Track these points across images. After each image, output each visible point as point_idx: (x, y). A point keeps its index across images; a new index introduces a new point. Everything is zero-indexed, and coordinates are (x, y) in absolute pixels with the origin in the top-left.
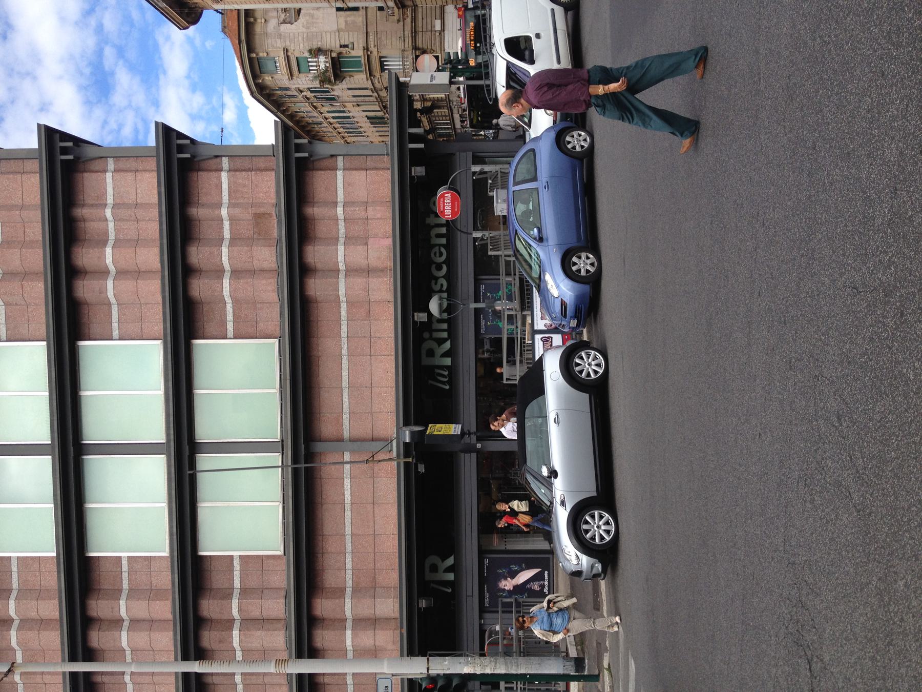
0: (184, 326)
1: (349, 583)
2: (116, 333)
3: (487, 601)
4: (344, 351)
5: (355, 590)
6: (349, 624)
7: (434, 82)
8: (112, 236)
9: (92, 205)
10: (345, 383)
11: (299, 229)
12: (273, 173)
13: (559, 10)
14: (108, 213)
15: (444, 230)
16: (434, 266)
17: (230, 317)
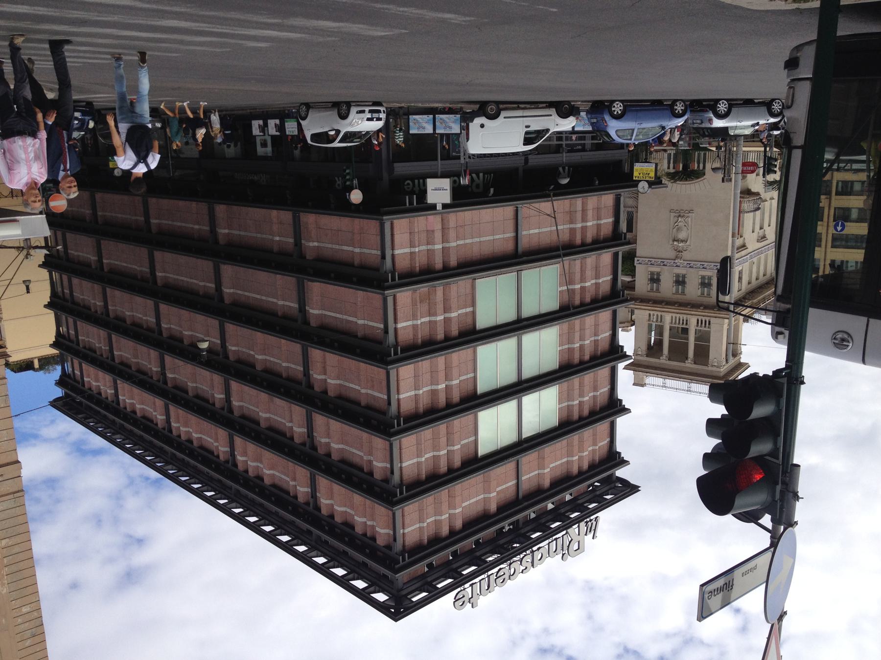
0: (473, 335)
1: (568, 226)
2: (472, 375)
3: (580, 147)
4: (478, 240)
5: (571, 222)
6: (584, 224)
7: (448, 188)
8: (429, 388)
9: (417, 402)
10: (491, 238)
11: (426, 274)
12: (398, 295)
13: (503, 114)
14: (421, 392)
15: (421, 181)
17: (464, 311)
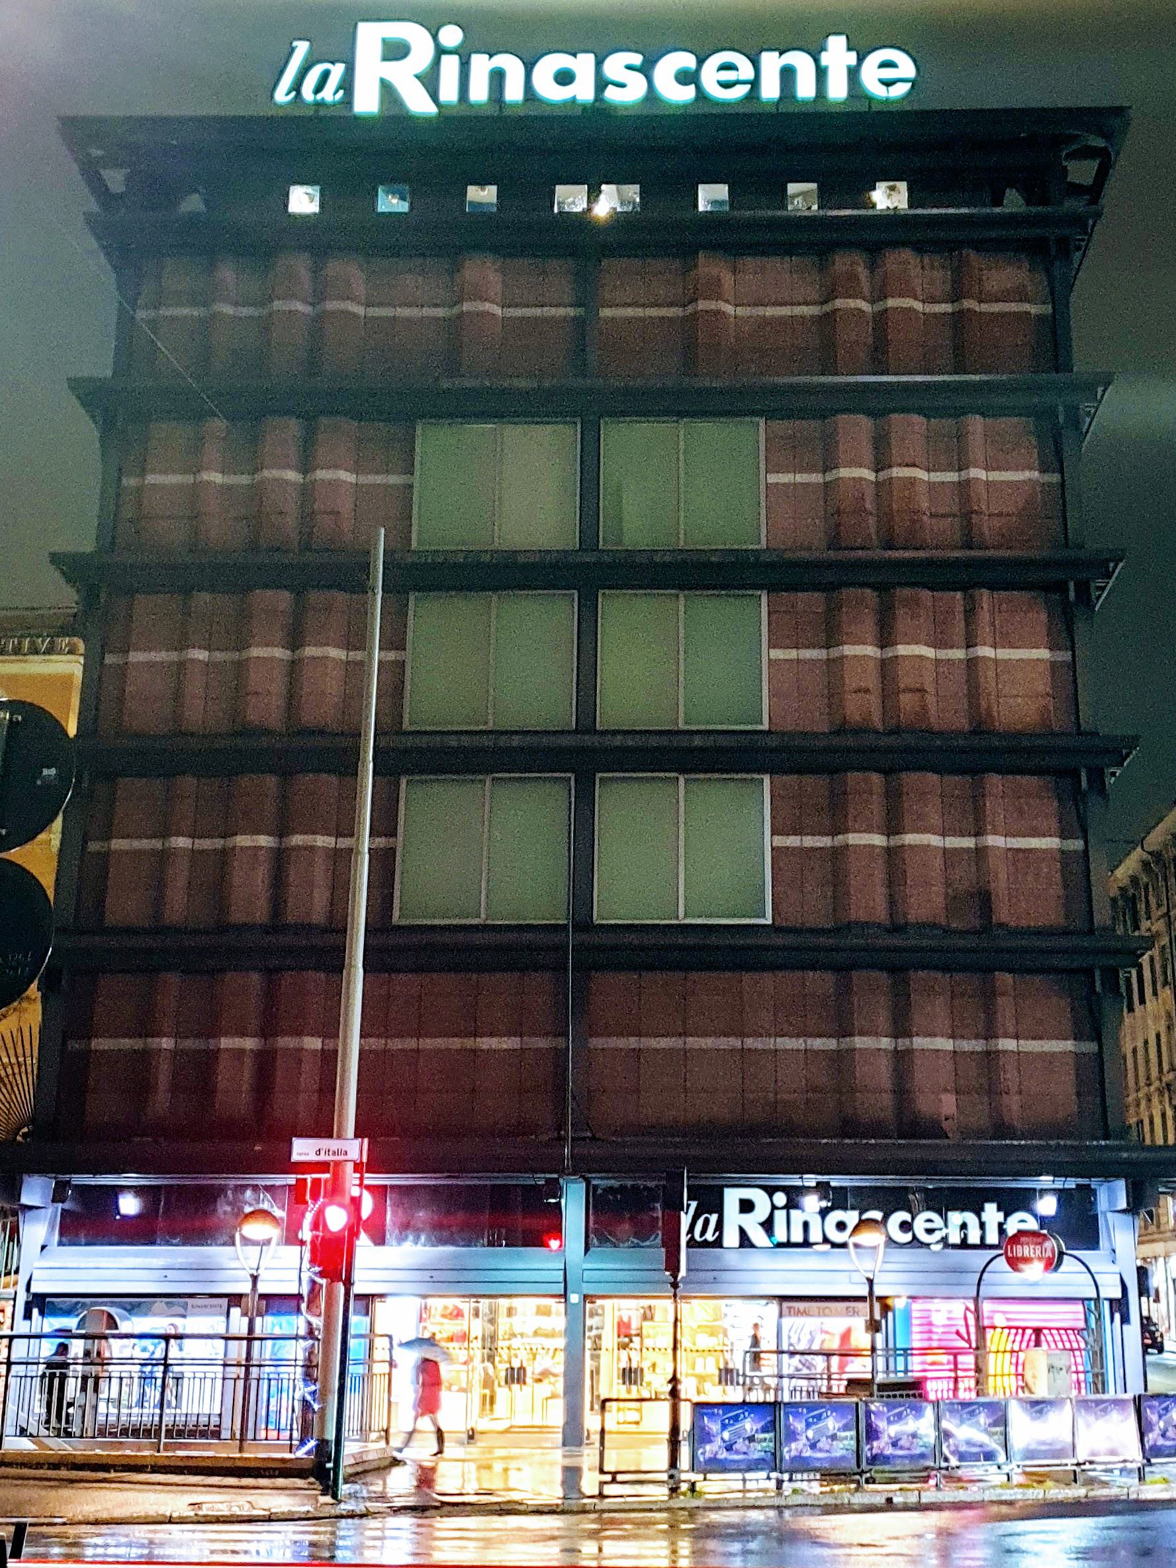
10: (693, 1042)
16: (906, 1216)
